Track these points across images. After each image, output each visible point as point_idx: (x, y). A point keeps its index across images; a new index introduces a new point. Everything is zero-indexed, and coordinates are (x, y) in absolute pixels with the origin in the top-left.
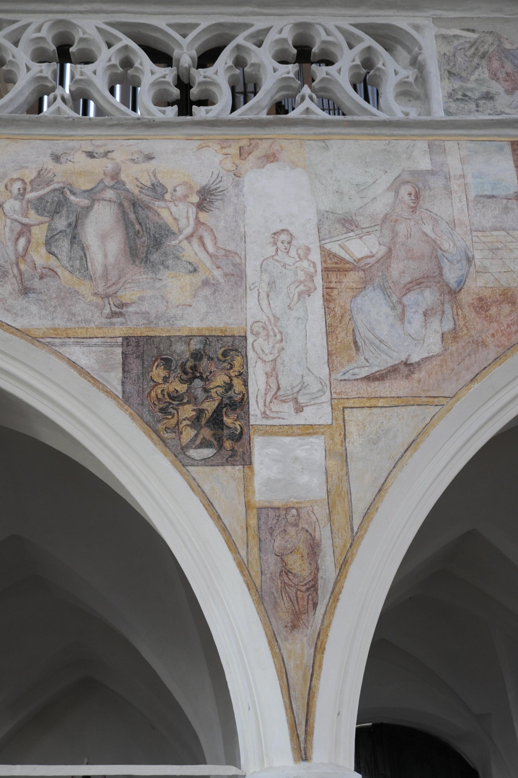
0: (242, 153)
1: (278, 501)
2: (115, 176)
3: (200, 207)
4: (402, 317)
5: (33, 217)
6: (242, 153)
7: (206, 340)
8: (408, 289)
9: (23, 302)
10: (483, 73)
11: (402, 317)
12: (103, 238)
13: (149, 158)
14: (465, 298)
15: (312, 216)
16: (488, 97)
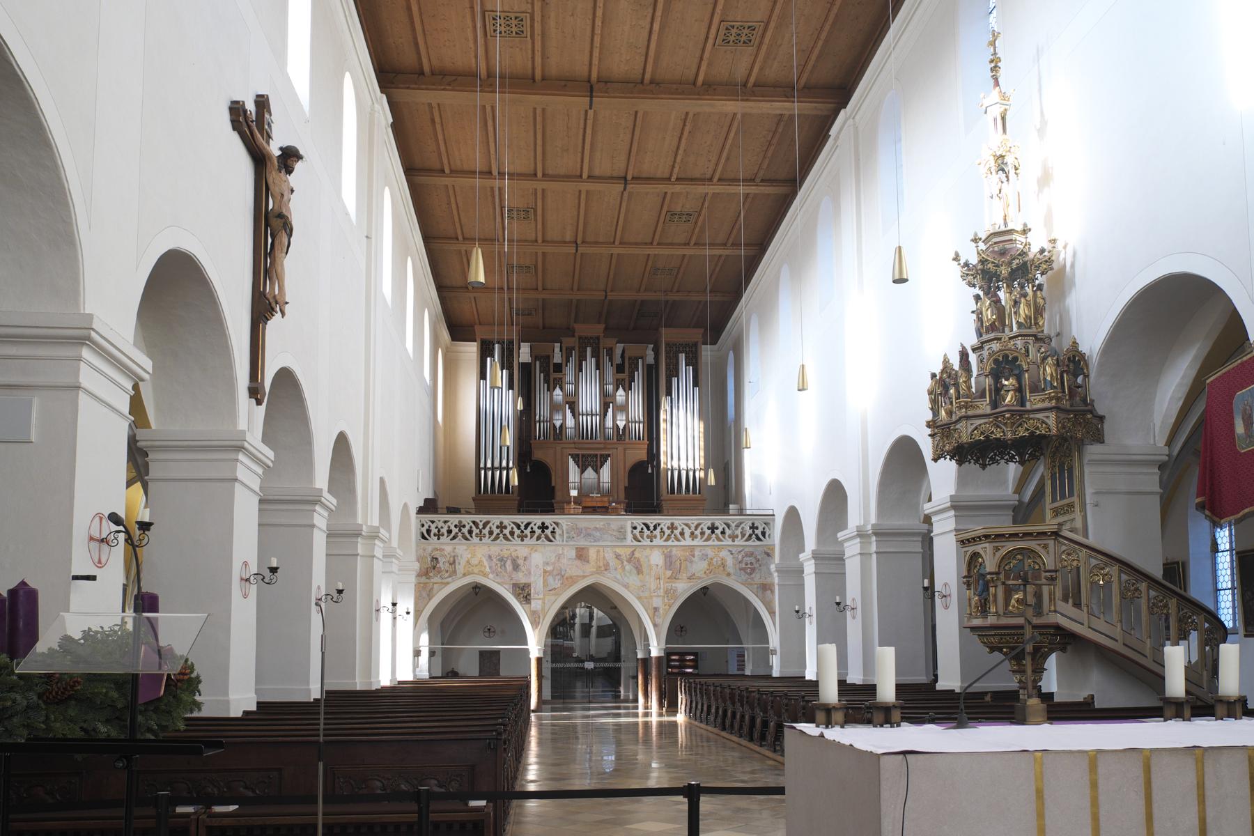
0: (532, 549)
1: (535, 609)
2: (511, 554)
3: (525, 560)
4: (555, 580)
5: (498, 562)
6: (532, 549)
7: (525, 584)
8: (556, 575)
9: (496, 577)
10: (573, 533)
11: (555, 580)
12: (509, 566)
13: (516, 550)
14: (565, 577)
15: (542, 562)
16: (573, 537)
